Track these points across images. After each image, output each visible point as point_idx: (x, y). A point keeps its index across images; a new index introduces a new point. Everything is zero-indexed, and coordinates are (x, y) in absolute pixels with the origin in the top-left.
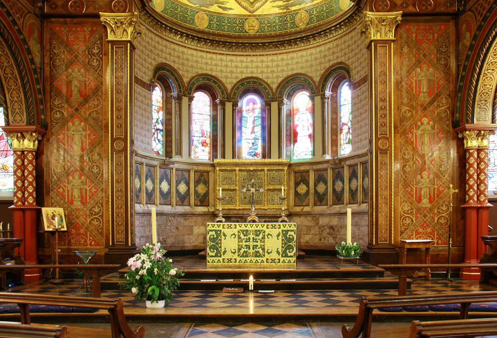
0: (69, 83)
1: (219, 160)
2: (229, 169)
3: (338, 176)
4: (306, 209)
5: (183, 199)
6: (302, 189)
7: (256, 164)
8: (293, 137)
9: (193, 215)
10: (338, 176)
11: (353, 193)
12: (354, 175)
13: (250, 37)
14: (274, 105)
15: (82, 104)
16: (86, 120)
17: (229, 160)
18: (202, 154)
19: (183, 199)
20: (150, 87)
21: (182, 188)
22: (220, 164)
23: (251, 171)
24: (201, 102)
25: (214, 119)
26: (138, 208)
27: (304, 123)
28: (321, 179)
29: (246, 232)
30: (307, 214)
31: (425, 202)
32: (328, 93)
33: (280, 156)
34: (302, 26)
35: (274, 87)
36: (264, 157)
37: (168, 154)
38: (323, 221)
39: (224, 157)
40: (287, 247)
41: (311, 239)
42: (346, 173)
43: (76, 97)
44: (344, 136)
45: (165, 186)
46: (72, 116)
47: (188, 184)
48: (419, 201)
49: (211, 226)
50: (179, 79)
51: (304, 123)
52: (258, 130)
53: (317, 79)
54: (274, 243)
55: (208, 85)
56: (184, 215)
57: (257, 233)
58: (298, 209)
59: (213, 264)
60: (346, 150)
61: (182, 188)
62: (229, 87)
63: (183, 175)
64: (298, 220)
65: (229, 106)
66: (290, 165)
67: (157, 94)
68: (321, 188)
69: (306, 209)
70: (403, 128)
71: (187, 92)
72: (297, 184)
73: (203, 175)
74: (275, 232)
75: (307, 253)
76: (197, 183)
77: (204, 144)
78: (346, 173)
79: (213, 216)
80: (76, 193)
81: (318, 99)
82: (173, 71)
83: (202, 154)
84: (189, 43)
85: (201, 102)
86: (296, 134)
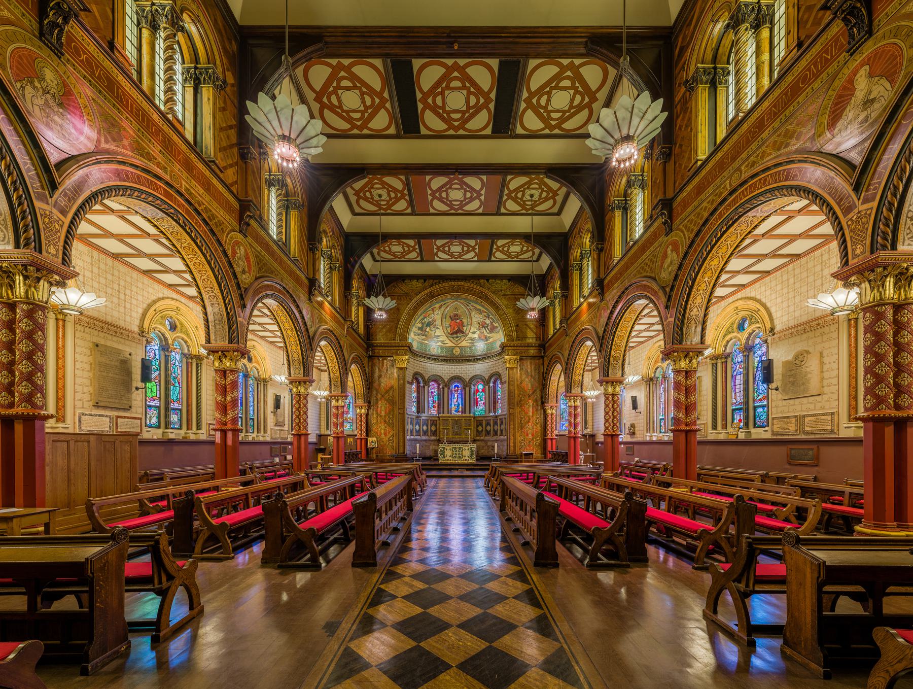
0: (380, 384)
1: (441, 415)
2: (446, 421)
3: (496, 423)
4: (482, 438)
5: (425, 433)
6: (480, 428)
7: (459, 417)
8: (476, 403)
9: (429, 440)
10: (496, 423)
11: (502, 431)
12: (502, 423)
13: (456, 357)
14: (467, 389)
15: (385, 394)
16: (387, 400)
17: (446, 415)
18: (434, 412)
19: (425, 433)
20: (411, 383)
21: (425, 428)
22: (442, 417)
23: (457, 422)
24: (433, 388)
25: (439, 394)
26: (408, 437)
27: (481, 396)
28: (488, 424)
29: (455, 448)
30: (482, 440)
31: (530, 436)
32: (491, 385)
33: (470, 413)
34: (480, 353)
35: (467, 380)
36: (462, 413)
37: (418, 412)
38: (489, 443)
39: (444, 413)
40: (472, 454)
41: (484, 452)
42: (499, 422)
43: (383, 391)
44: (499, 405)
45: (417, 427)
46: (381, 399)
47: (427, 426)
48: (527, 435)
49: (440, 445)
50: (423, 378)
51: (481, 396)
52: (460, 401)
53: (487, 378)
54: (466, 453)
55: (437, 379)
56: (425, 440)
57: (460, 448)
58: (478, 438)
59: (442, 460)
60: (500, 412)
61: (425, 428)
62: (446, 380)
63: (426, 423)
64: (478, 443)
65: (446, 389)
66: (474, 417)
67: (414, 386)
68: (488, 428)
69: (482, 438)
70: (520, 404)
71: (426, 383)
72: (478, 426)
73: (434, 422)
74: (467, 448)
75: (480, 458)
76: (431, 425)
77: (434, 407)
78: (499, 422)
79: (439, 441)
80: (383, 431)
81: (487, 387)
82: (421, 375)
83: (434, 412)
84: (428, 361)
85: (433, 388)
86: (477, 402)
